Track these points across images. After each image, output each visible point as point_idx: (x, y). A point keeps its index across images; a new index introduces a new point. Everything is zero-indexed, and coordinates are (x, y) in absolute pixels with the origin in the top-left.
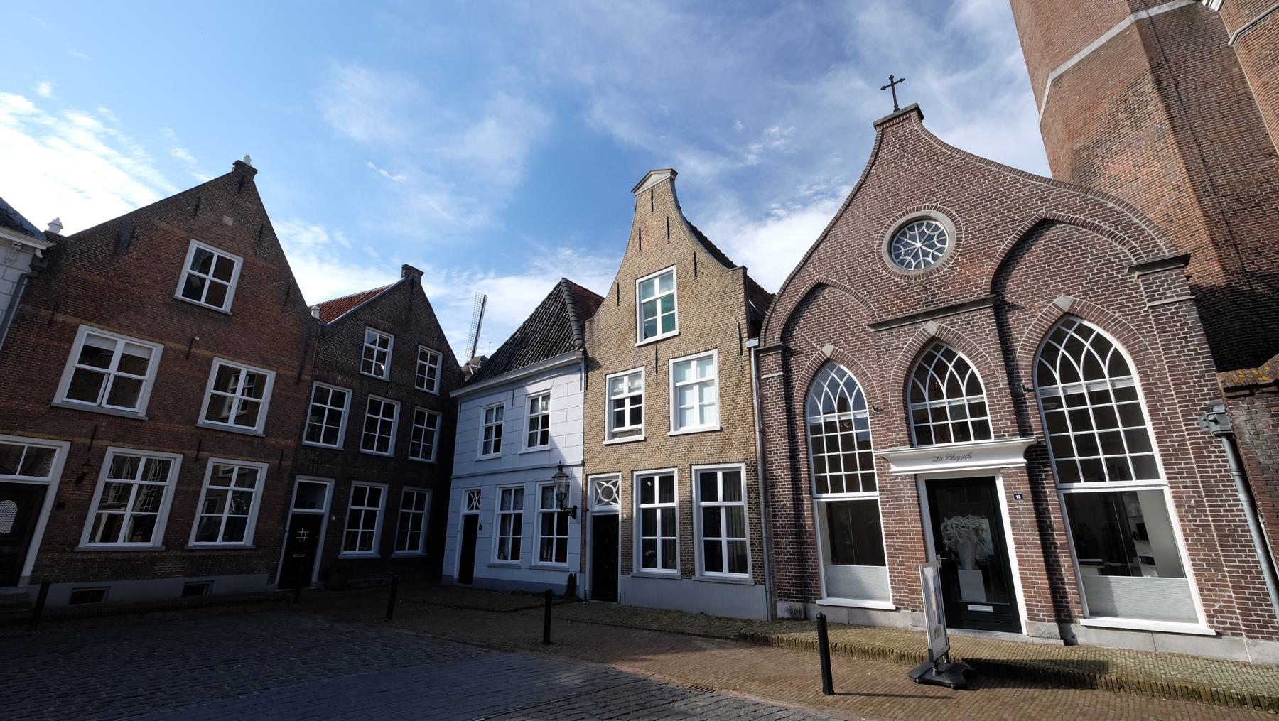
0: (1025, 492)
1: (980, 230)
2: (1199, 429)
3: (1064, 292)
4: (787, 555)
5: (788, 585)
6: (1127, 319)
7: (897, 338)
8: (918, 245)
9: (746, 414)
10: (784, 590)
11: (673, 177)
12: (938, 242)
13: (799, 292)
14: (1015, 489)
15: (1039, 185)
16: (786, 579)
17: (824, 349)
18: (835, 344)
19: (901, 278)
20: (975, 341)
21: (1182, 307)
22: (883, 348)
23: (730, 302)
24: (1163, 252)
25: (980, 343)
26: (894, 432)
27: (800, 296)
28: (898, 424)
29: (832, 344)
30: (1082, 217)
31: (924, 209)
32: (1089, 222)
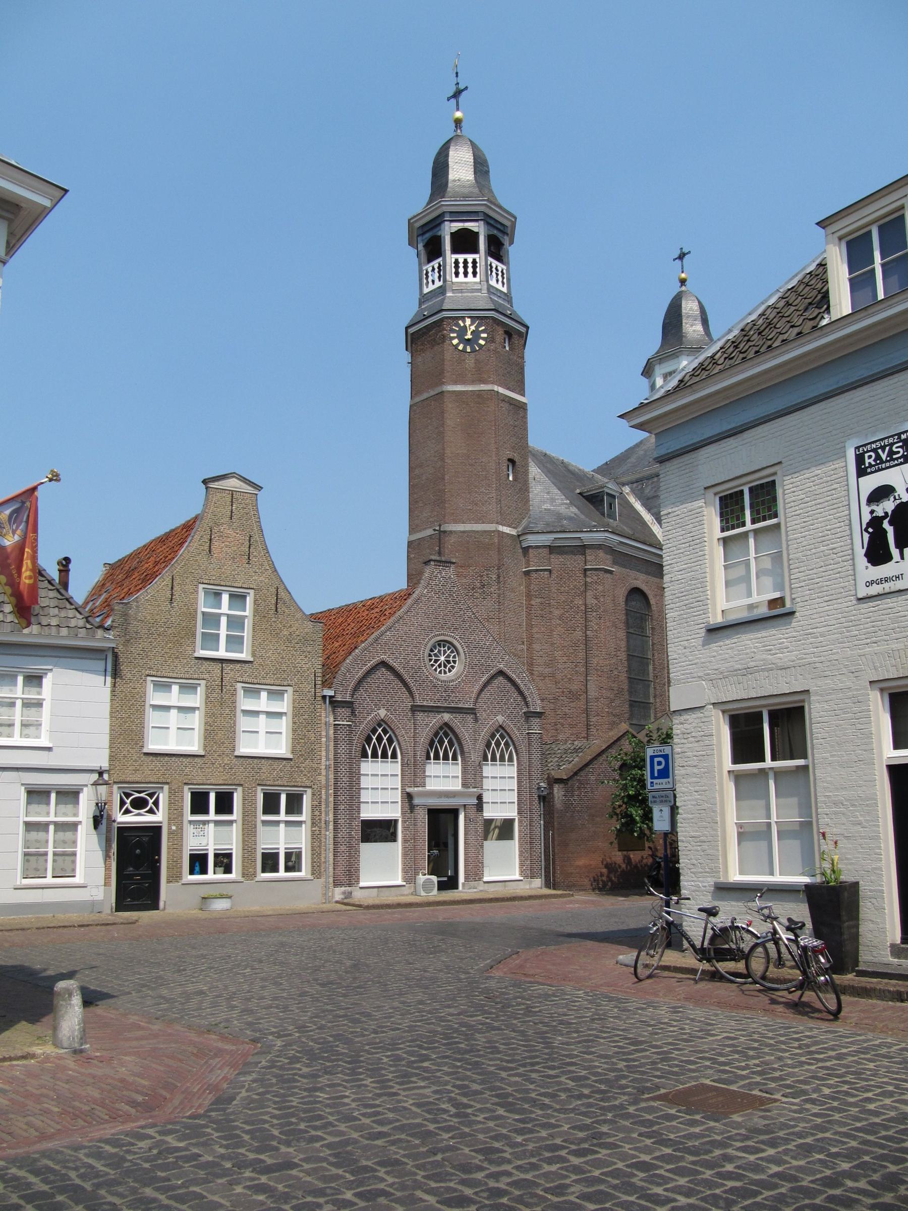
23: (309, 649)
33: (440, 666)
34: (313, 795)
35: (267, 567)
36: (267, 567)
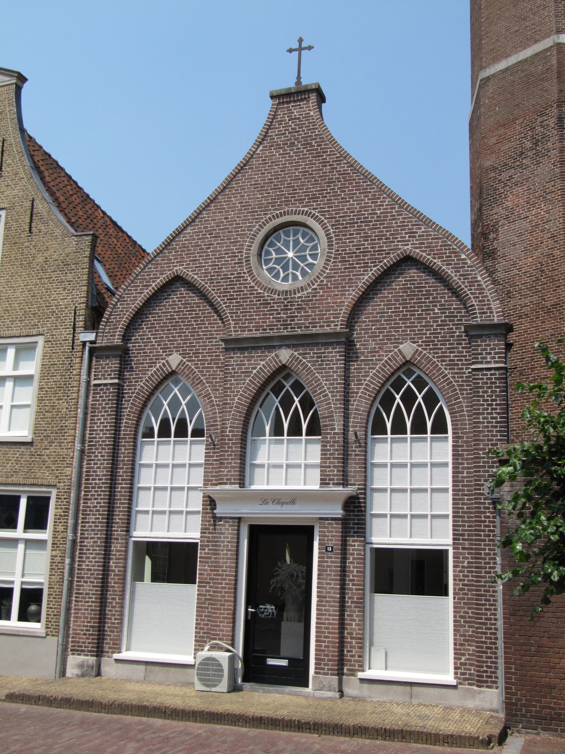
0: (336, 545)
1: (350, 253)
2: (482, 494)
3: (411, 339)
4: (88, 602)
5: (84, 637)
6: (454, 377)
7: (248, 361)
8: (290, 254)
9: (66, 426)
10: (79, 642)
11: (19, 84)
12: (310, 255)
13: (153, 282)
14: (328, 540)
15: (410, 218)
16: (82, 630)
17: (170, 359)
18: (183, 355)
19: (264, 290)
20: (322, 377)
21: (495, 374)
22: (233, 369)
23: (70, 277)
24: (493, 316)
25: (326, 380)
26: (226, 468)
27: (153, 288)
28: (232, 459)
29: (180, 354)
30: (440, 263)
31: (299, 214)
32: (444, 270)
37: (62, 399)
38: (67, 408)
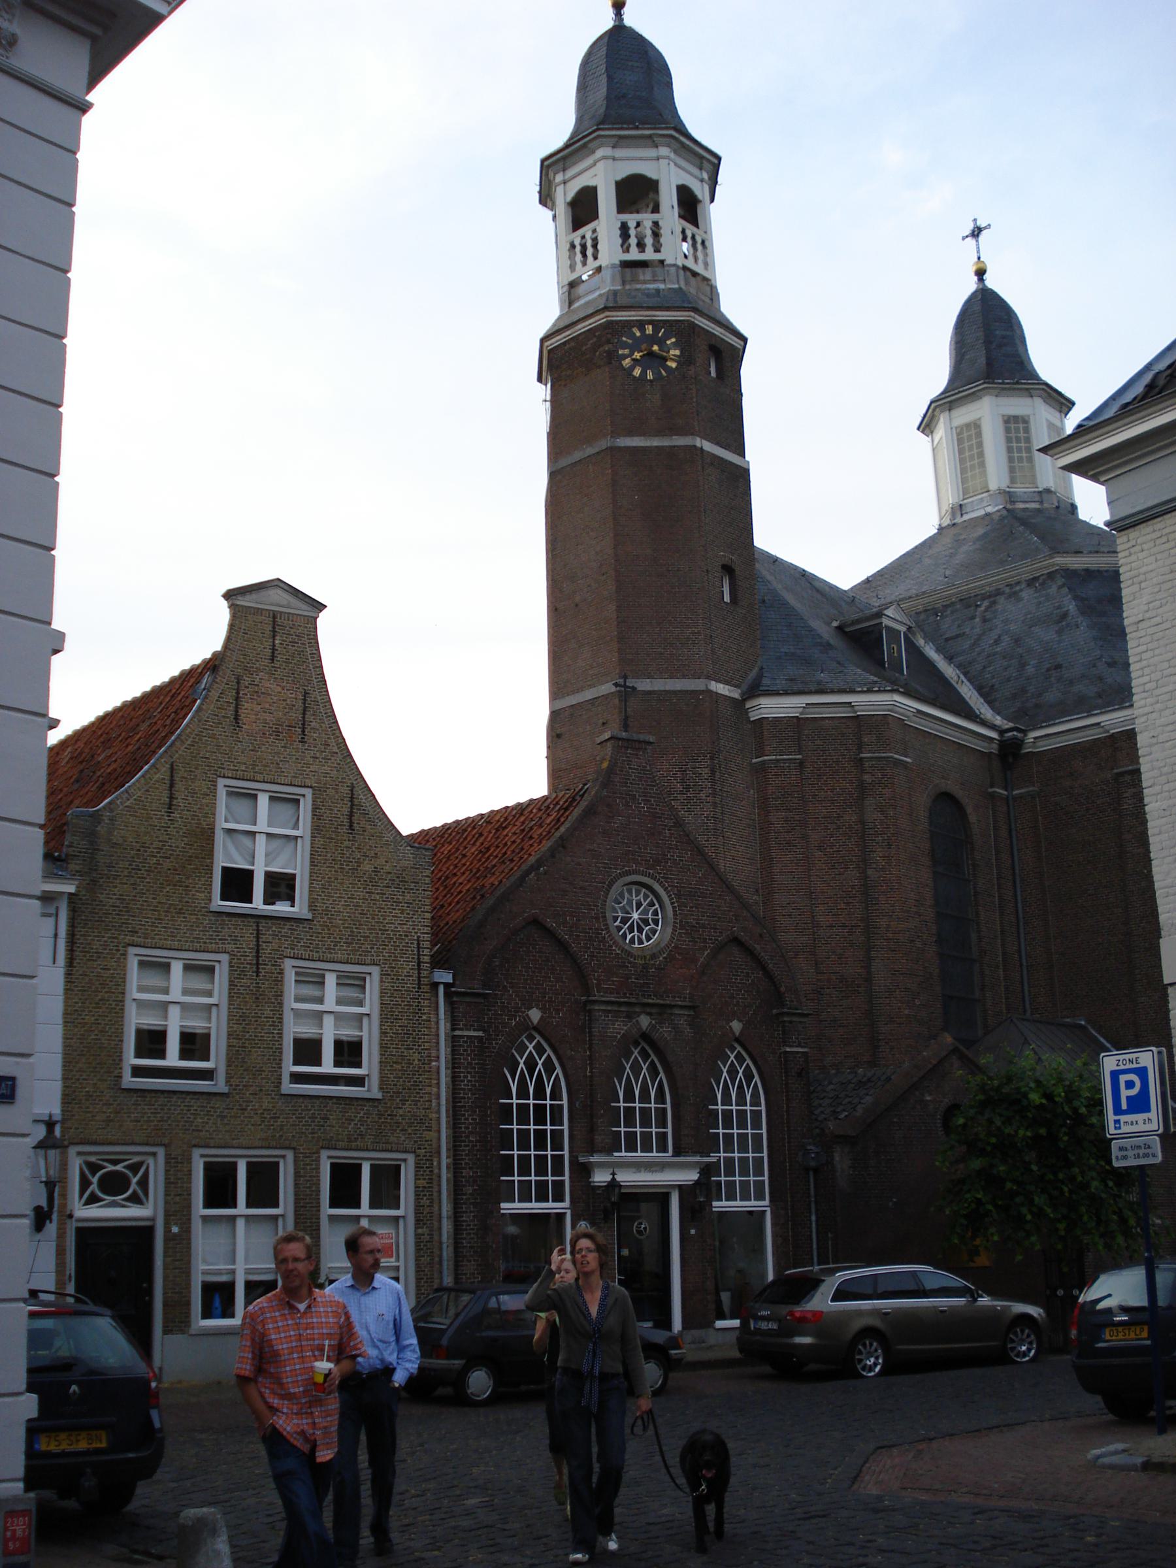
8: (635, 916)
9: (420, 1082)
33: (631, 929)
34: (418, 1167)
35: (335, 749)
36: (335, 749)
37: (412, 1049)
38: (419, 1060)
